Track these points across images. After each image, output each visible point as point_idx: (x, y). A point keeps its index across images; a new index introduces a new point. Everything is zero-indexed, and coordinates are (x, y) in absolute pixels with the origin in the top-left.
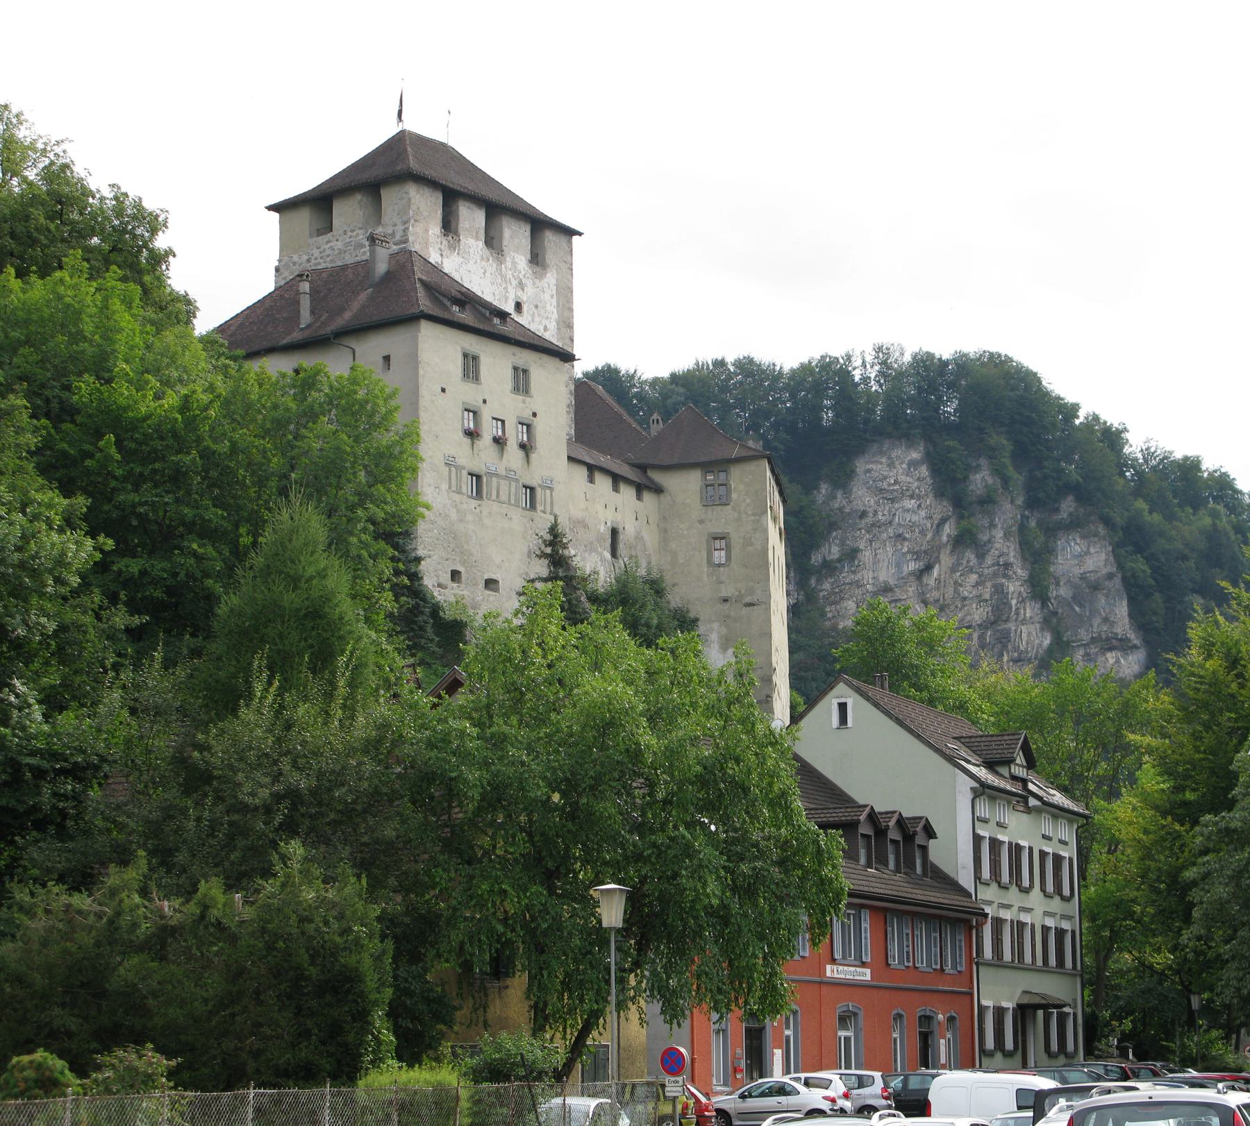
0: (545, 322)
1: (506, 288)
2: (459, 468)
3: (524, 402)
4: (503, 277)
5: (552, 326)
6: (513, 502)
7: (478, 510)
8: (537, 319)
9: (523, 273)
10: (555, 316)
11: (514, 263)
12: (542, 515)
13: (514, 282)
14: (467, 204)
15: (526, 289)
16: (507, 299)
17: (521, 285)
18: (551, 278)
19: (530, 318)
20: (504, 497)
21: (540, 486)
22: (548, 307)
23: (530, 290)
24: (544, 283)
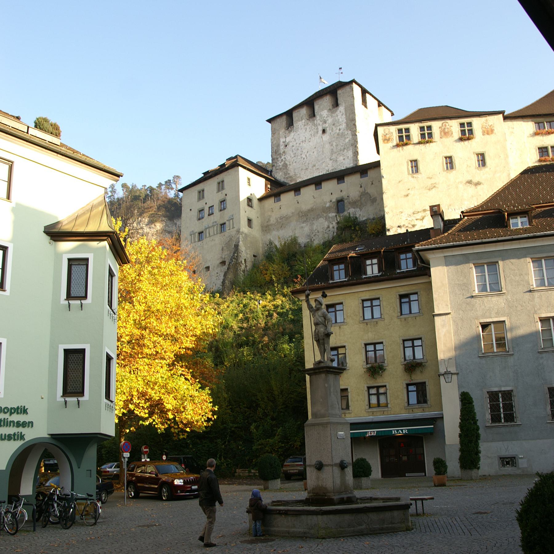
0: (341, 127)
1: (317, 129)
2: (194, 234)
3: (222, 193)
4: (316, 125)
5: (344, 126)
6: (215, 233)
7: (202, 244)
8: (334, 129)
9: (326, 116)
10: (345, 121)
11: (321, 116)
12: (229, 231)
13: (321, 123)
14: (297, 111)
15: (327, 122)
16: (317, 132)
17: (325, 122)
18: (341, 108)
19: (331, 131)
20: (212, 234)
21: (227, 221)
22: (340, 120)
23: (330, 120)
24: (338, 112)
